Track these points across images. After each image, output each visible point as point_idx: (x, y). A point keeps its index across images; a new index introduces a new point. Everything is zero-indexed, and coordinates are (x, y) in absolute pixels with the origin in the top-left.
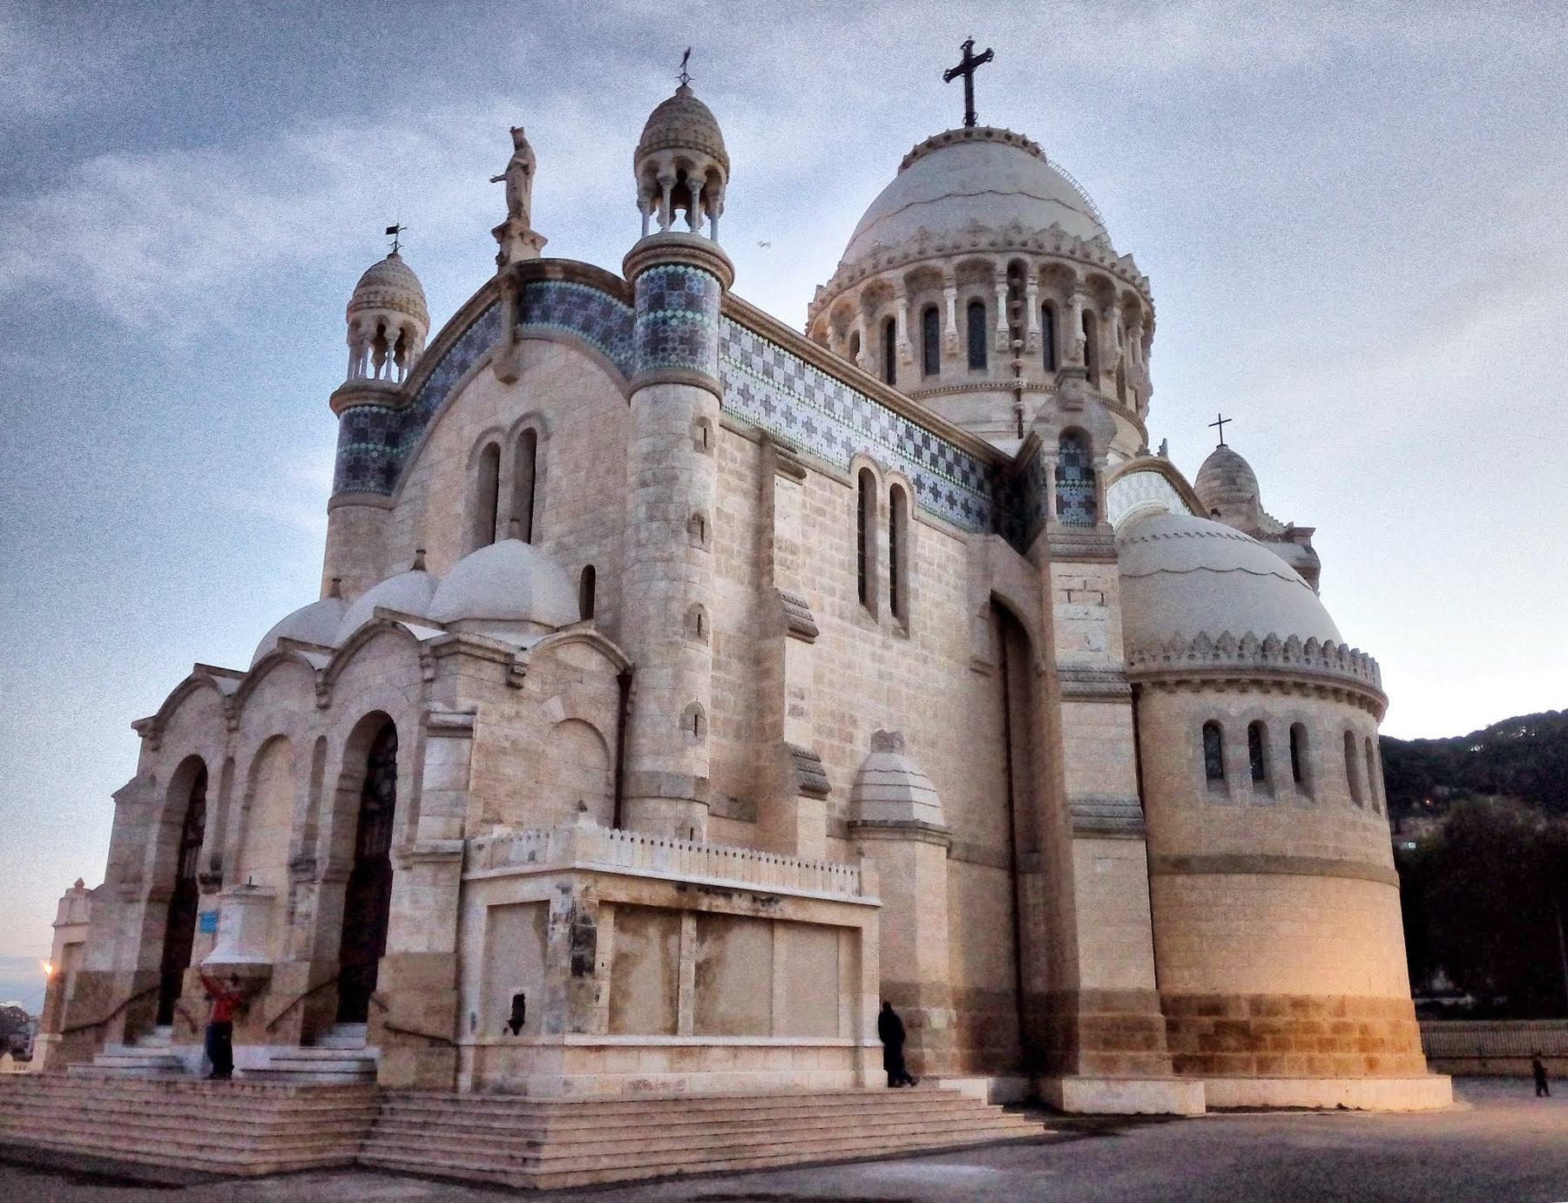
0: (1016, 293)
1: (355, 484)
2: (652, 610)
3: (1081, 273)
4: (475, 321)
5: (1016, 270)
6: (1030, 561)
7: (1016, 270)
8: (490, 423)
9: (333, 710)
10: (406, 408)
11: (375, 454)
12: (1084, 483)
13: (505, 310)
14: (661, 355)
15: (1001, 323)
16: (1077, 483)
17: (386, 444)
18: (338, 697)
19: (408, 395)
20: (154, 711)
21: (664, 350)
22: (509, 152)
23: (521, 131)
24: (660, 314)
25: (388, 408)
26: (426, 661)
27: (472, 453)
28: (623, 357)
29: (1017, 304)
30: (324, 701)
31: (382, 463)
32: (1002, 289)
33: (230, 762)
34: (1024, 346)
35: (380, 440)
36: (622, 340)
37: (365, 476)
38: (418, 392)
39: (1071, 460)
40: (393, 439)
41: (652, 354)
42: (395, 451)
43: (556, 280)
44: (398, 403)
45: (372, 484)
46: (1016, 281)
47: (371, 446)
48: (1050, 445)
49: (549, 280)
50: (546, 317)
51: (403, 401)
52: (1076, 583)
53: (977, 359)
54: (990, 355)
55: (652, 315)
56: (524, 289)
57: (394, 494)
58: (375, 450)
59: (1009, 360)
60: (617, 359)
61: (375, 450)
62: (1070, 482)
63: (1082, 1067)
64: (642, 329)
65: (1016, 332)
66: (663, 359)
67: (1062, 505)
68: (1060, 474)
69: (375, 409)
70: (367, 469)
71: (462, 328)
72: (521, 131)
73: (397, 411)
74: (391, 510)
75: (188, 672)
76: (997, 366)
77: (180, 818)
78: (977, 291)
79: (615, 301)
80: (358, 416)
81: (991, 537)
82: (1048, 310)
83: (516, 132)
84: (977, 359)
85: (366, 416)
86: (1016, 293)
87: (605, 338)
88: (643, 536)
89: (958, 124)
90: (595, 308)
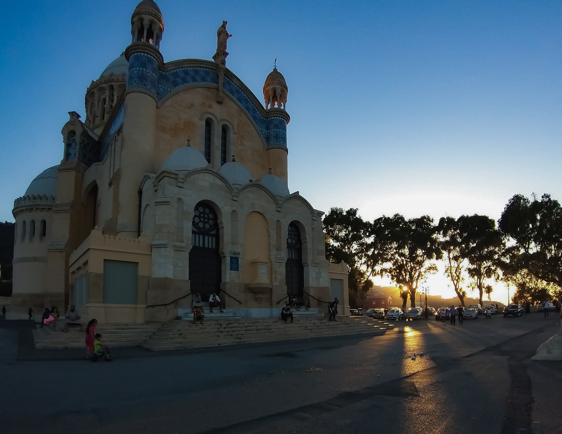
38: (170, 71)
83: (225, 23)
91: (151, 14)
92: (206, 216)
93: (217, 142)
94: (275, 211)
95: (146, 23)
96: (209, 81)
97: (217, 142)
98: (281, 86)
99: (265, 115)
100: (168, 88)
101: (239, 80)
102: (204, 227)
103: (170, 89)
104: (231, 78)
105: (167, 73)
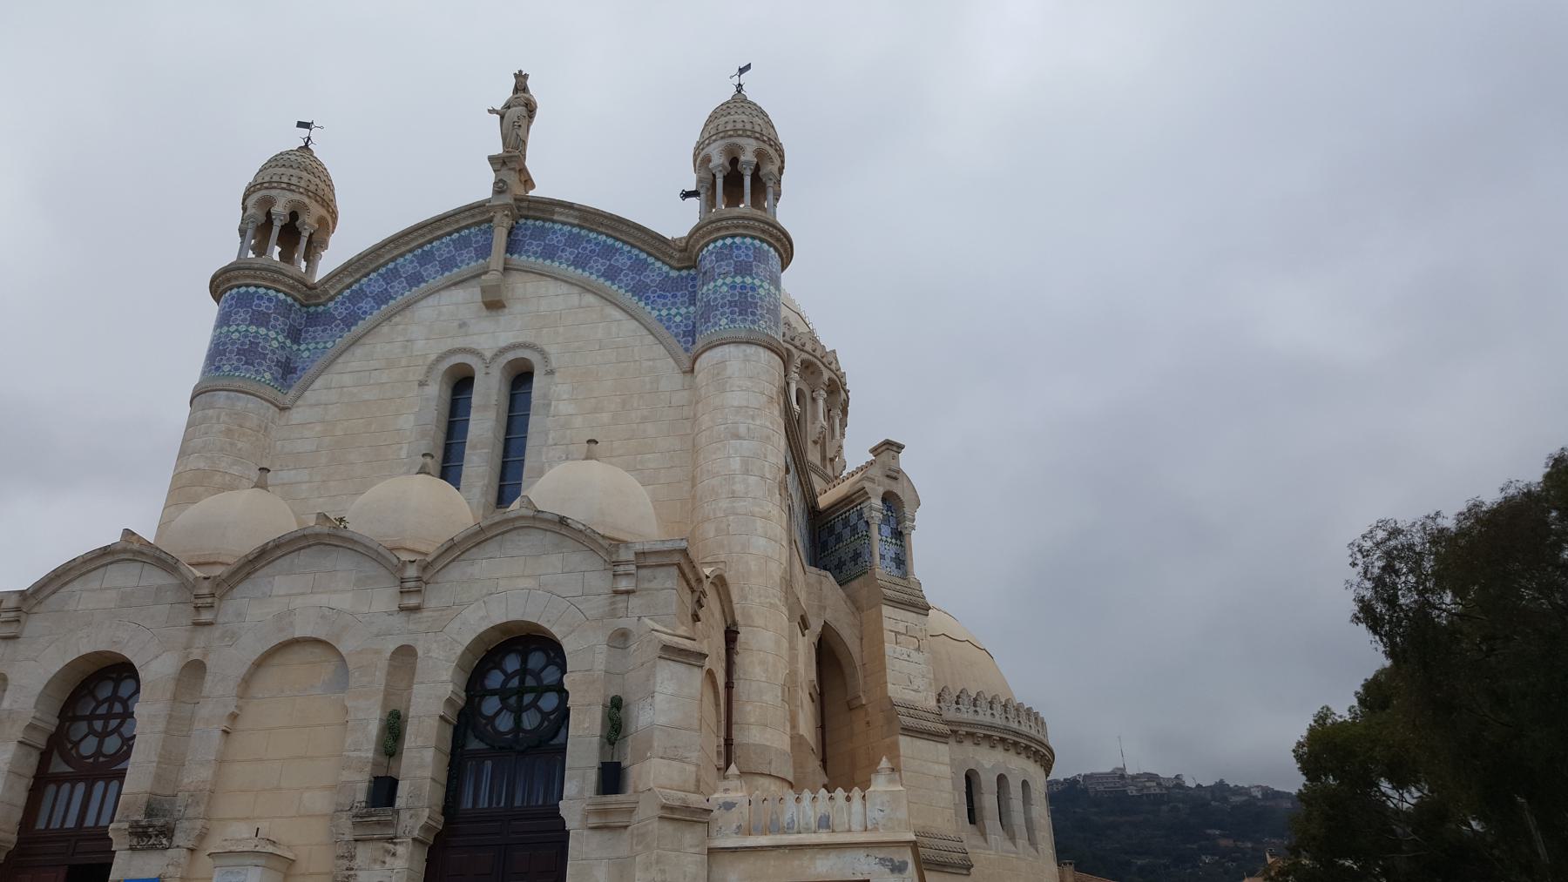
1: (248, 370)
2: (753, 566)
3: (826, 375)
4: (439, 238)
6: (853, 600)
8: (459, 343)
9: (425, 614)
10: (317, 305)
11: (275, 344)
12: (894, 541)
13: (500, 238)
14: (751, 318)
16: (889, 540)
17: (286, 338)
18: (434, 599)
19: (326, 292)
20: (25, 584)
21: (753, 314)
22: (507, 92)
23: (526, 76)
24: (748, 280)
25: (295, 299)
26: (621, 569)
27: (430, 369)
28: (664, 313)
30: (413, 601)
31: (281, 355)
33: (195, 670)
35: (283, 331)
36: (665, 297)
37: (260, 364)
38: (340, 292)
39: (886, 520)
40: (295, 335)
41: (740, 314)
42: (295, 347)
43: (564, 223)
44: (308, 297)
45: (268, 376)
47: (272, 334)
48: (877, 502)
49: (554, 222)
50: (550, 253)
51: (318, 296)
52: (901, 628)
55: (738, 279)
56: (517, 223)
57: (292, 393)
58: (276, 339)
60: (655, 313)
61: (276, 339)
64: (725, 289)
66: (753, 322)
67: (882, 557)
69: (282, 296)
70: (264, 356)
71: (421, 241)
72: (526, 76)
73: (302, 305)
74: (283, 409)
75: (112, 537)
77: (41, 742)
79: (651, 260)
80: (260, 298)
81: (823, 572)
85: (270, 300)
87: (639, 290)
88: (739, 488)
90: (622, 261)
91: (289, 187)
92: (102, 710)
93: (483, 425)
94: (390, 614)
95: (280, 210)
96: (467, 261)
97: (483, 425)
98: (722, 138)
99: (679, 260)
100: (325, 343)
101: (570, 206)
102: (99, 752)
103: (334, 342)
104: (548, 216)
105: (331, 304)
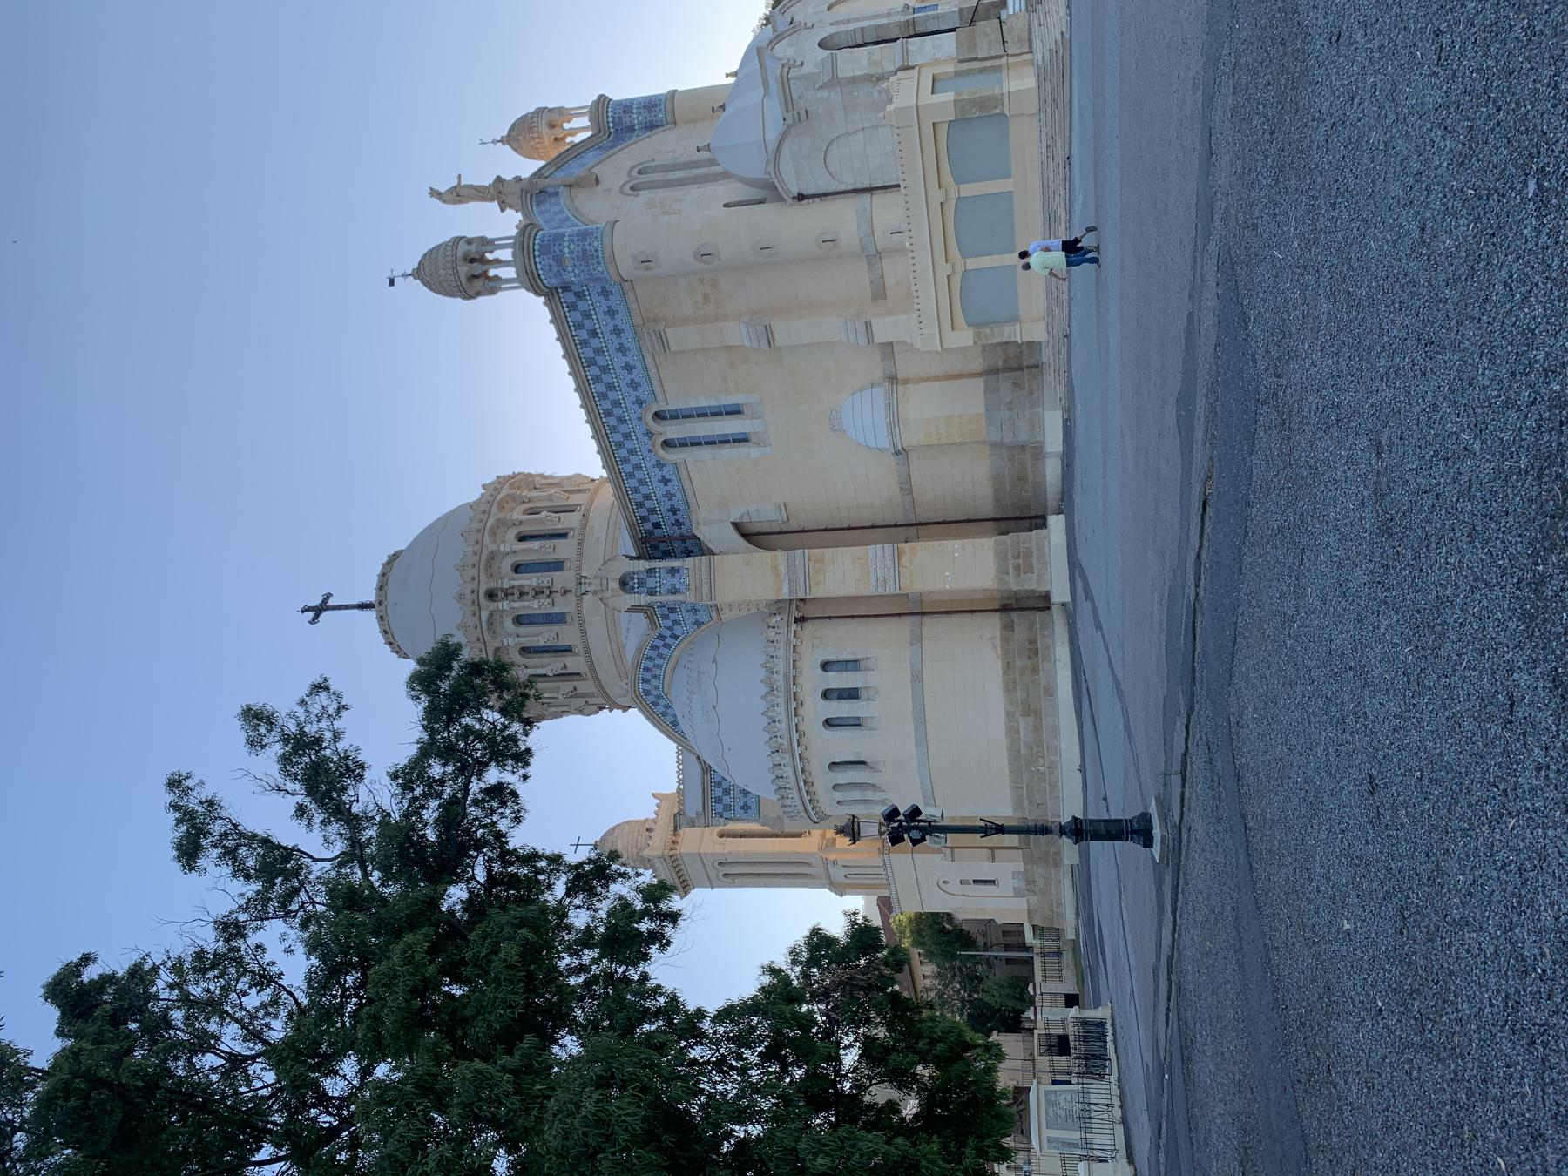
0: (507, 594)
5: (491, 595)
7: (491, 595)
12: (657, 575)
15: (534, 606)
29: (517, 593)
32: (505, 605)
34: (548, 588)
46: (501, 595)
53: (559, 619)
54: (556, 610)
59: (557, 597)
62: (658, 584)
63: (1046, 589)
65: (538, 593)
67: (674, 591)
68: (652, 592)
76: (562, 605)
78: (508, 623)
82: (517, 569)
84: (559, 619)
86: (507, 594)
89: (371, 614)
